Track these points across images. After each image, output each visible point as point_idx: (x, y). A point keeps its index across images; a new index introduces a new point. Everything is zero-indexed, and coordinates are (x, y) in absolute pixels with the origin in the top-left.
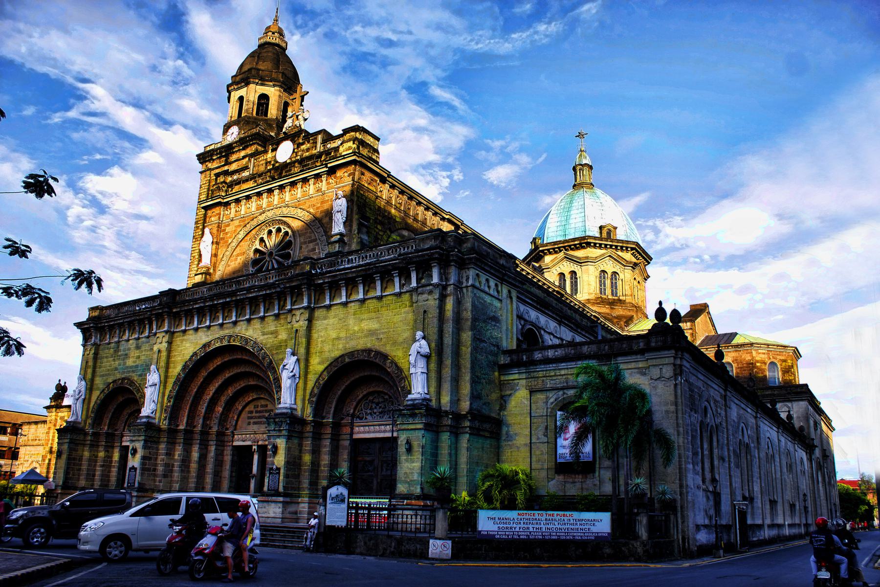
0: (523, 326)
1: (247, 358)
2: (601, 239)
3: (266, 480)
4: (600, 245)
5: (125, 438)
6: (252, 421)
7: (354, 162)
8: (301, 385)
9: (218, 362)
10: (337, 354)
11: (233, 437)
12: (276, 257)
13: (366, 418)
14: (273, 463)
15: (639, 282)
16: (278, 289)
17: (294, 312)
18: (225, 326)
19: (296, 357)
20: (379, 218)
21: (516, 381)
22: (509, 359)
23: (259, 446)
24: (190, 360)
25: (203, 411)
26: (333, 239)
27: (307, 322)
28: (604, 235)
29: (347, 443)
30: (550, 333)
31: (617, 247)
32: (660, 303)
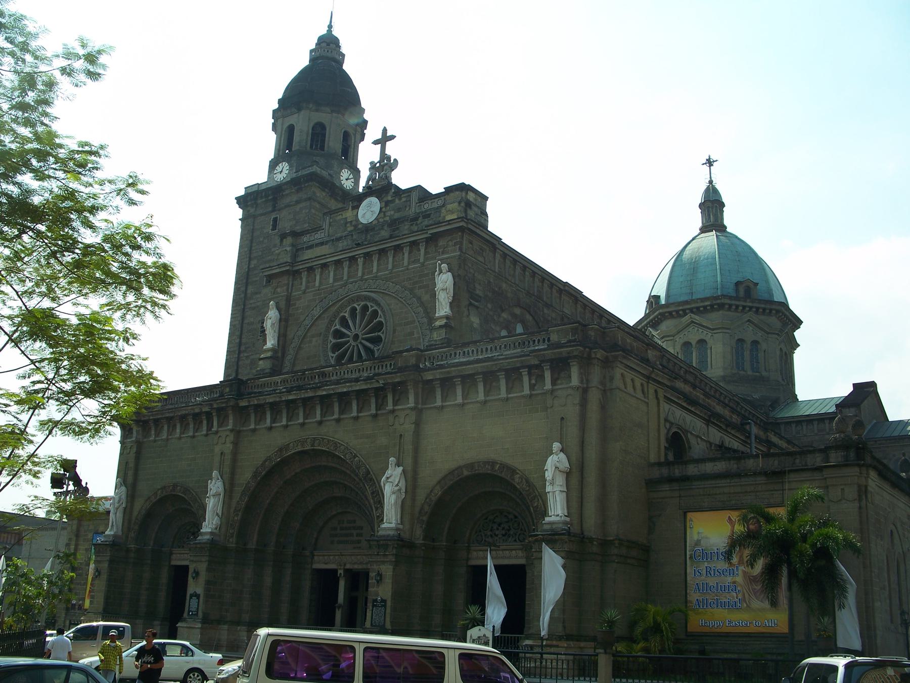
0: (669, 430)
2: (737, 298)
3: (369, 614)
5: (174, 556)
7: (461, 229)
12: (363, 341)
14: (377, 595)
15: (786, 353)
19: (401, 468)
23: (347, 571)
26: (438, 323)
27: (413, 426)
28: (742, 293)
30: (697, 437)
31: (758, 309)
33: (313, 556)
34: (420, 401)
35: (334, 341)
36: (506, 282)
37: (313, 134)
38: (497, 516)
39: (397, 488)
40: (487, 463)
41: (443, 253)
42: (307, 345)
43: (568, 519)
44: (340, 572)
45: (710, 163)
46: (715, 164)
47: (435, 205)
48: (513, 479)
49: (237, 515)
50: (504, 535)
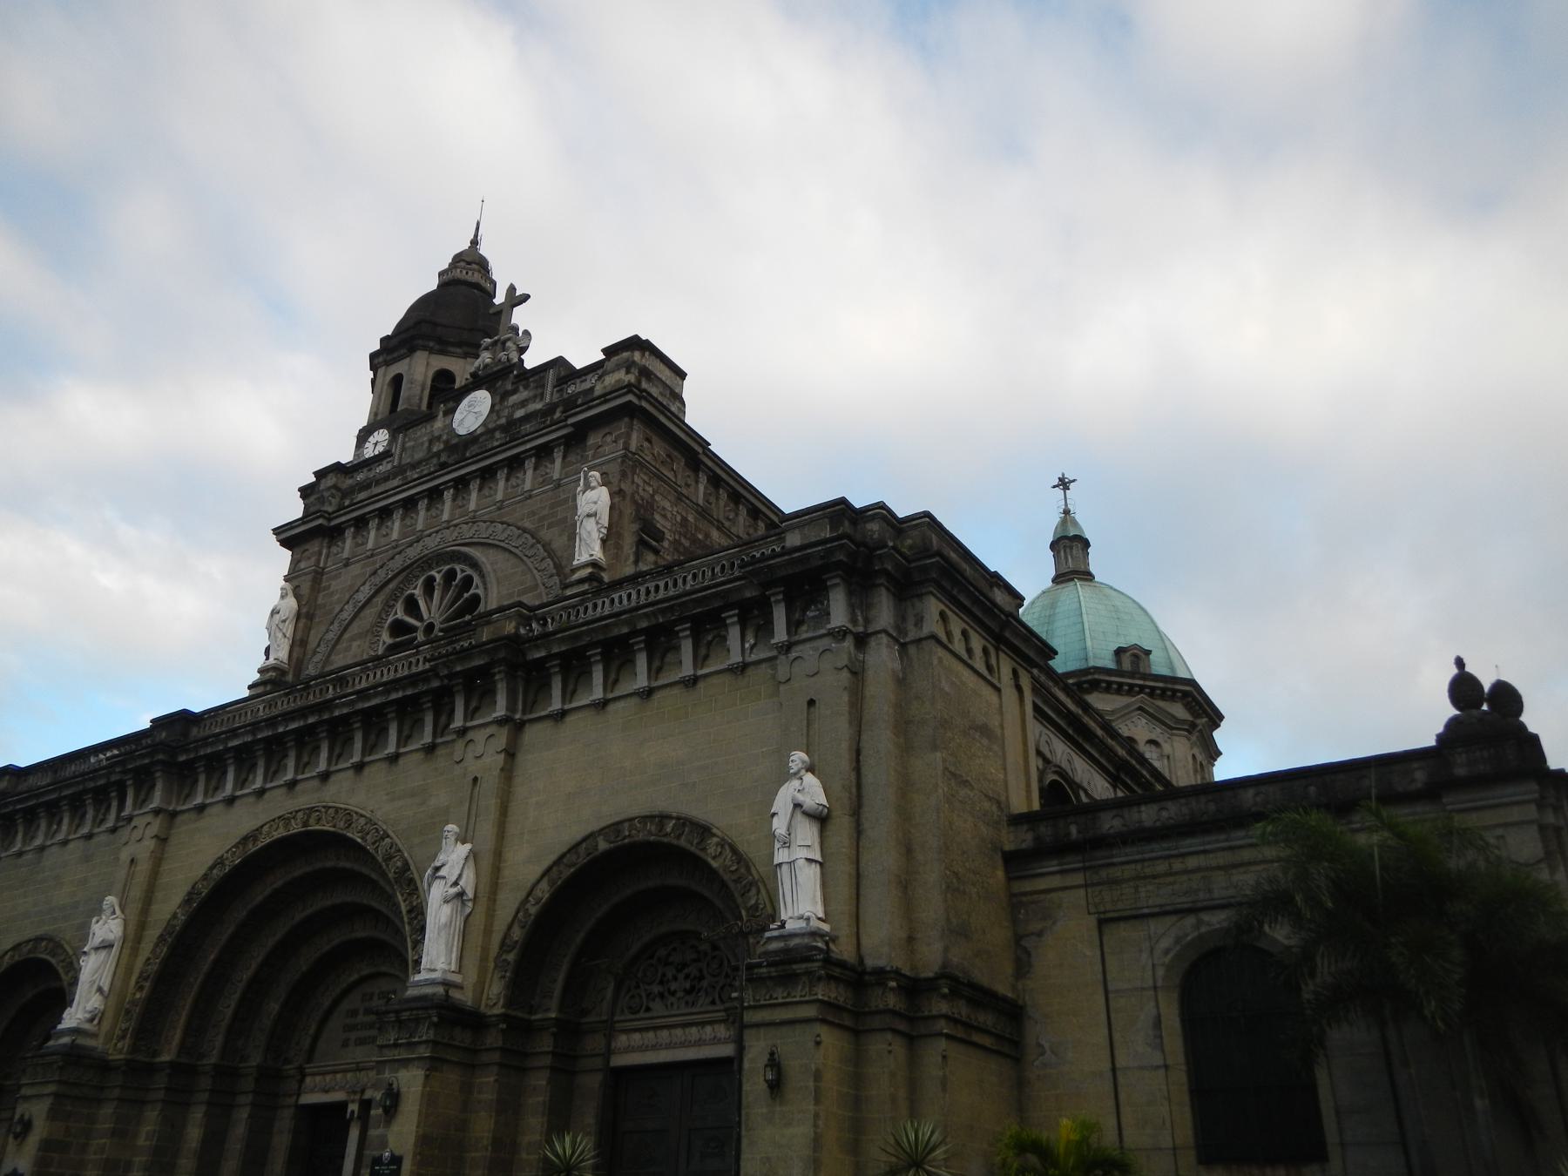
1: (348, 865)
4: (1120, 685)
6: (353, 1035)
7: (628, 411)
8: (479, 920)
9: (277, 880)
10: (576, 833)
11: (302, 1081)
13: (648, 1009)
14: (384, 1144)
15: (1201, 764)
16: (435, 684)
17: (470, 735)
18: (299, 788)
19: (464, 849)
20: (683, 540)
21: (1054, 895)
22: (1029, 836)
24: (205, 877)
25: (229, 1013)
26: (577, 576)
27: (502, 756)
28: (1127, 666)
29: (592, 1082)
31: (1153, 689)
32: (1460, 663)
33: (303, 1076)
34: (520, 707)
35: (389, 641)
36: (718, 528)
37: (433, 387)
38: (674, 949)
39: (454, 890)
40: (645, 819)
41: (594, 457)
42: (341, 656)
43: (826, 927)
44: (353, 1107)
45: (1064, 484)
46: (1072, 486)
47: (587, 385)
48: (704, 849)
49: (141, 988)
50: (688, 992)
